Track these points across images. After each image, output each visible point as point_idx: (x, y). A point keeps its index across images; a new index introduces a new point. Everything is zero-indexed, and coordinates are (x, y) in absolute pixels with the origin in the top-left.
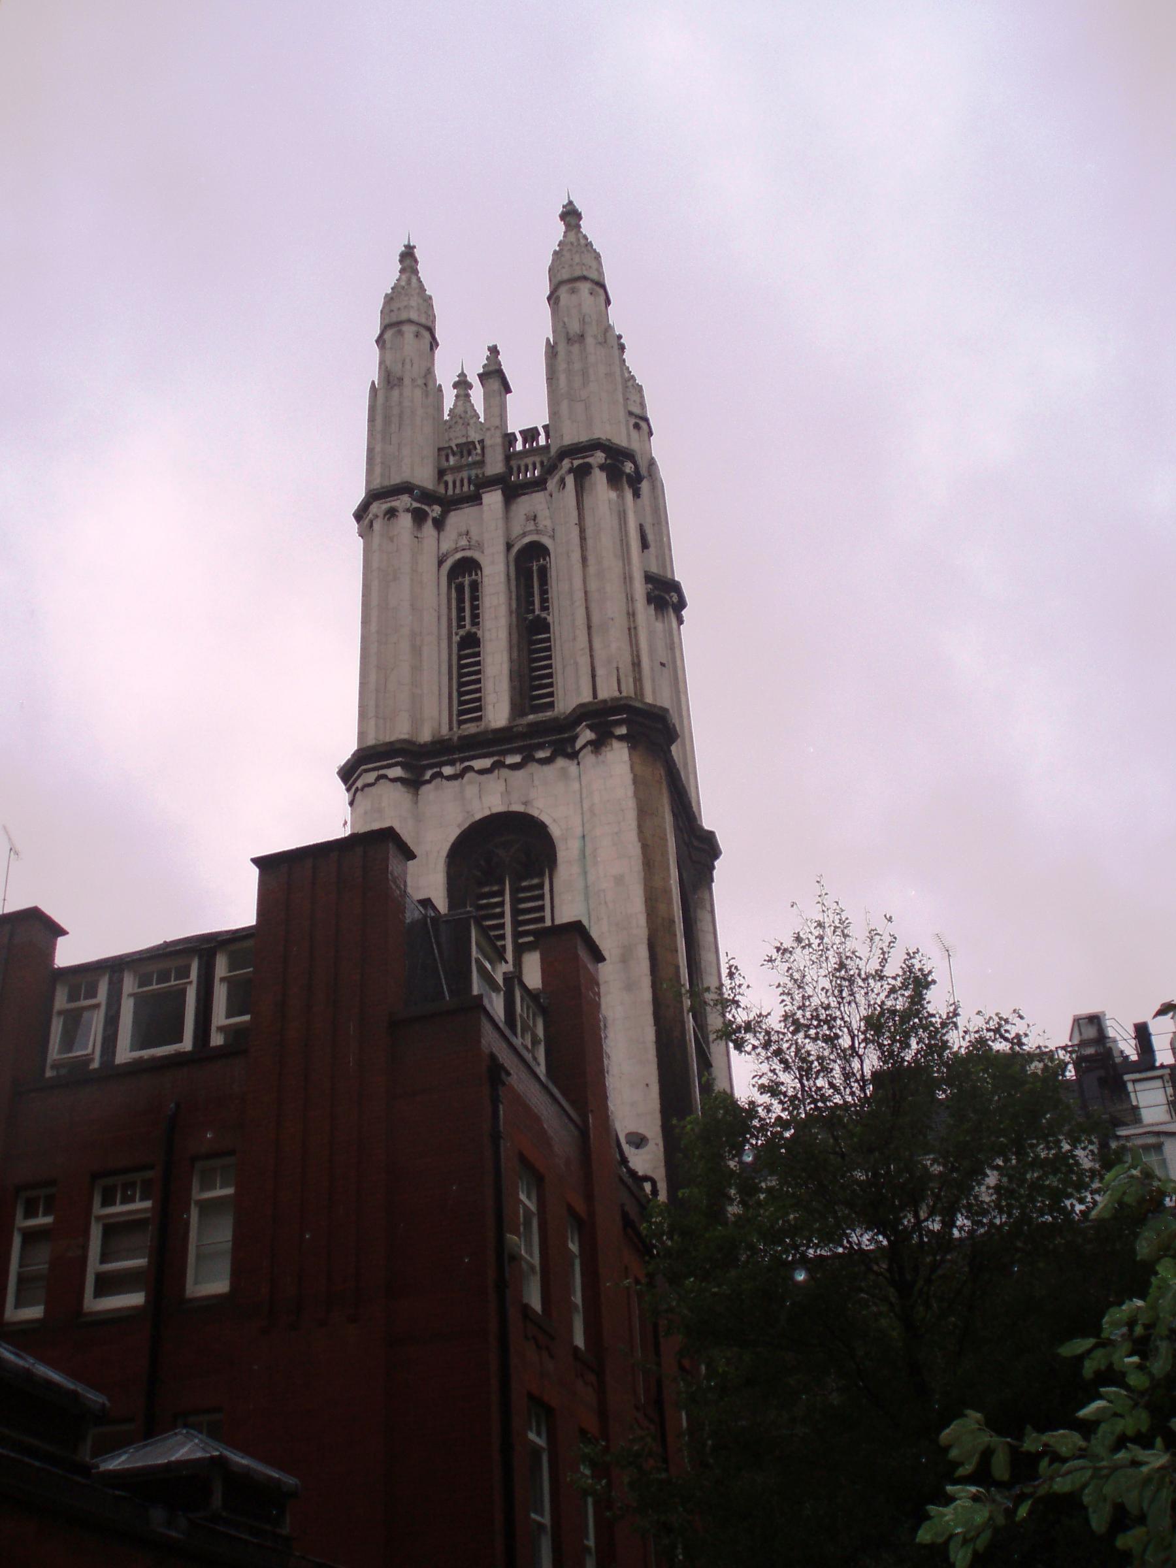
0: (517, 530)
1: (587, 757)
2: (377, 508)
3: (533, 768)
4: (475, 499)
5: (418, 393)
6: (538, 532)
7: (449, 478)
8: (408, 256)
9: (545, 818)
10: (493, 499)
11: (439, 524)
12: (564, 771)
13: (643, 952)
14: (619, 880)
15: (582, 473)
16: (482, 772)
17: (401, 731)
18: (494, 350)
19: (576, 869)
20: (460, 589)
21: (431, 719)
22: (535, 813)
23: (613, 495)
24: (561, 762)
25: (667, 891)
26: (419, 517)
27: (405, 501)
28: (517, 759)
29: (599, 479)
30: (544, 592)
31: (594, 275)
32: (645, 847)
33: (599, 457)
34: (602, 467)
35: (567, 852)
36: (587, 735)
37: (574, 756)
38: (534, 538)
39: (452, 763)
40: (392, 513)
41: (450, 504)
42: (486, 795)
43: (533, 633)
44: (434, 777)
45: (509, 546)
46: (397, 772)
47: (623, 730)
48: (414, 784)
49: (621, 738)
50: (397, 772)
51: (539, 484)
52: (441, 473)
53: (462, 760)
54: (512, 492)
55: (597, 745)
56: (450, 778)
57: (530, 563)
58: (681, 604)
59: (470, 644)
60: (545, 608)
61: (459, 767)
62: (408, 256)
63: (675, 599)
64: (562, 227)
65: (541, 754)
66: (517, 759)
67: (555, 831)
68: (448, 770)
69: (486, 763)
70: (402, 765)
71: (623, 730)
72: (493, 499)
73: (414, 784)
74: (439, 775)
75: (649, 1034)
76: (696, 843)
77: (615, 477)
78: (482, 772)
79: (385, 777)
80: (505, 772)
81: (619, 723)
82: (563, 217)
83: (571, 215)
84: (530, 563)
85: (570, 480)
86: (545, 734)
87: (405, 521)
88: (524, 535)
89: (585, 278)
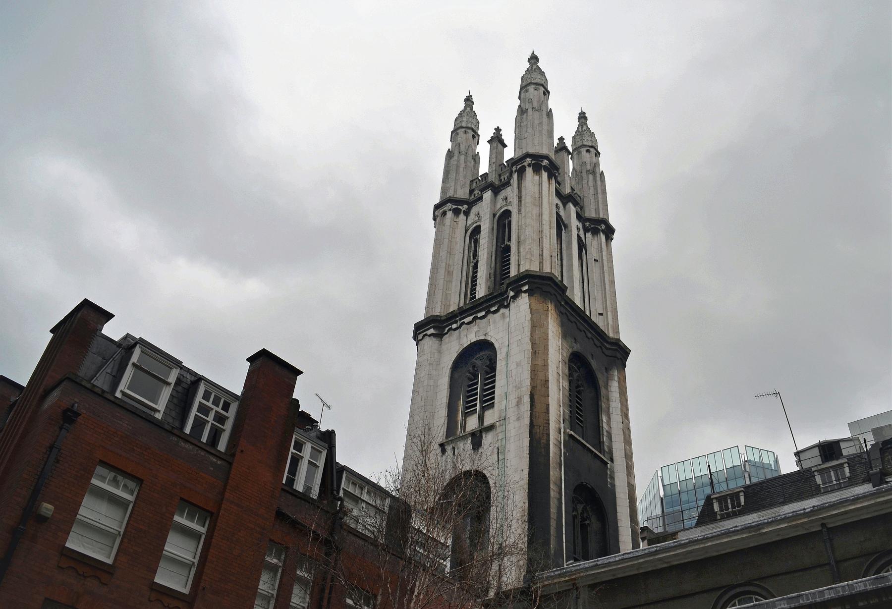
0: (499, 206)
1: (512, 305)
3: (490, 316)
5: (462, 158)
6: (507, 205)
7: (476, 192)
8: (469, 100)
9: (493, 340)
10: (488, 195)
11: (467, 213)
12: (503, 314)
13: (526, 400)
14: (519, 364)
15: (521, 172)
16: (469, 323)
17: (438, 311)
19: (504, 363)
22: (489, 338)
23: (537, 178)
24: (502, 311)
25: (545, 366)
26: (457, 212)
27: (449, 204)
28: (483, 313)
29: (529, 171)
31: (538, 81)
32: (533, 344)
33: (529, 160)
34: (529, 165)
35: (500, 356)
36: (512, 294)
37: (508, 306)
38: (506, 208)
39: (456, 322)
40: (444, 213)
41: (471, 204)
42: (470, 335)
43: (503, 253)
44: (448, 331)
45: (494, 215)
46: (432, 331)
47: (526, 288)
48: (440, 336)
49: (525, 292)
50: (432, 331)
51: (507, 184)
52: (471, 192)
53: (461, 319)
55: (515, 298)
56: (455, 329)
57: (503, 221)
58: (609, 232)
59: (476, 266)
60: (509, 240)
61: (459, 323)
63: (603, 227)
64: (527, 65)
65: (493, 309)
66: (483, 313)
67: (496, 346)
68: (454, 326)
69: (470, 318)
70: (434, 327)
71: (526, 288)
72: (488, 195)
73: (440, 336)
74: (451, 329)
75: (526, 442)
76: (607, 346)
77: (537, 169)
78: (469, 323)
79: (426, 335)
80: (478, 321)
81: (524, 285)
82: (529, 61)
83: (534, 59)
84: (503, 221)
85: (515, 176)
86: (498, 300)
87: (450, 214)
88: (501, 208)
89: (531, 84)
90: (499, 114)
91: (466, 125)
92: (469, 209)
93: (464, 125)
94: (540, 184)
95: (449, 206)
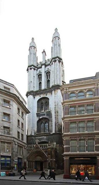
2: (29, 68)
4: (41, 67)
10: (43, 67)
11: (37, 70)
17: (32, 89)
18: (44, 50)
20: (39, 78)
21: (36, 89)
26: (34, 69)
30: (49, 77)
41: (38, 68)
54: (46, 66)
57: (48, 74)
62: (33, 39)
72: (43, 67)
77: (59, 62)
87: (33, 69)
90: (45, 45)
91: (33, 47)
92: (37, 69)
93: (34, 46)
94: (60, 65)
95: (30, 67)
